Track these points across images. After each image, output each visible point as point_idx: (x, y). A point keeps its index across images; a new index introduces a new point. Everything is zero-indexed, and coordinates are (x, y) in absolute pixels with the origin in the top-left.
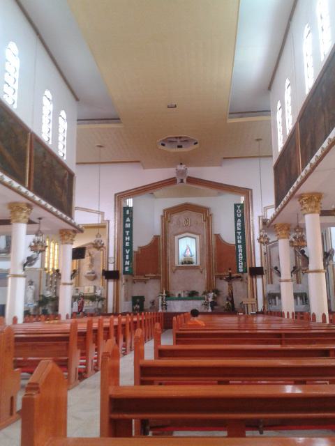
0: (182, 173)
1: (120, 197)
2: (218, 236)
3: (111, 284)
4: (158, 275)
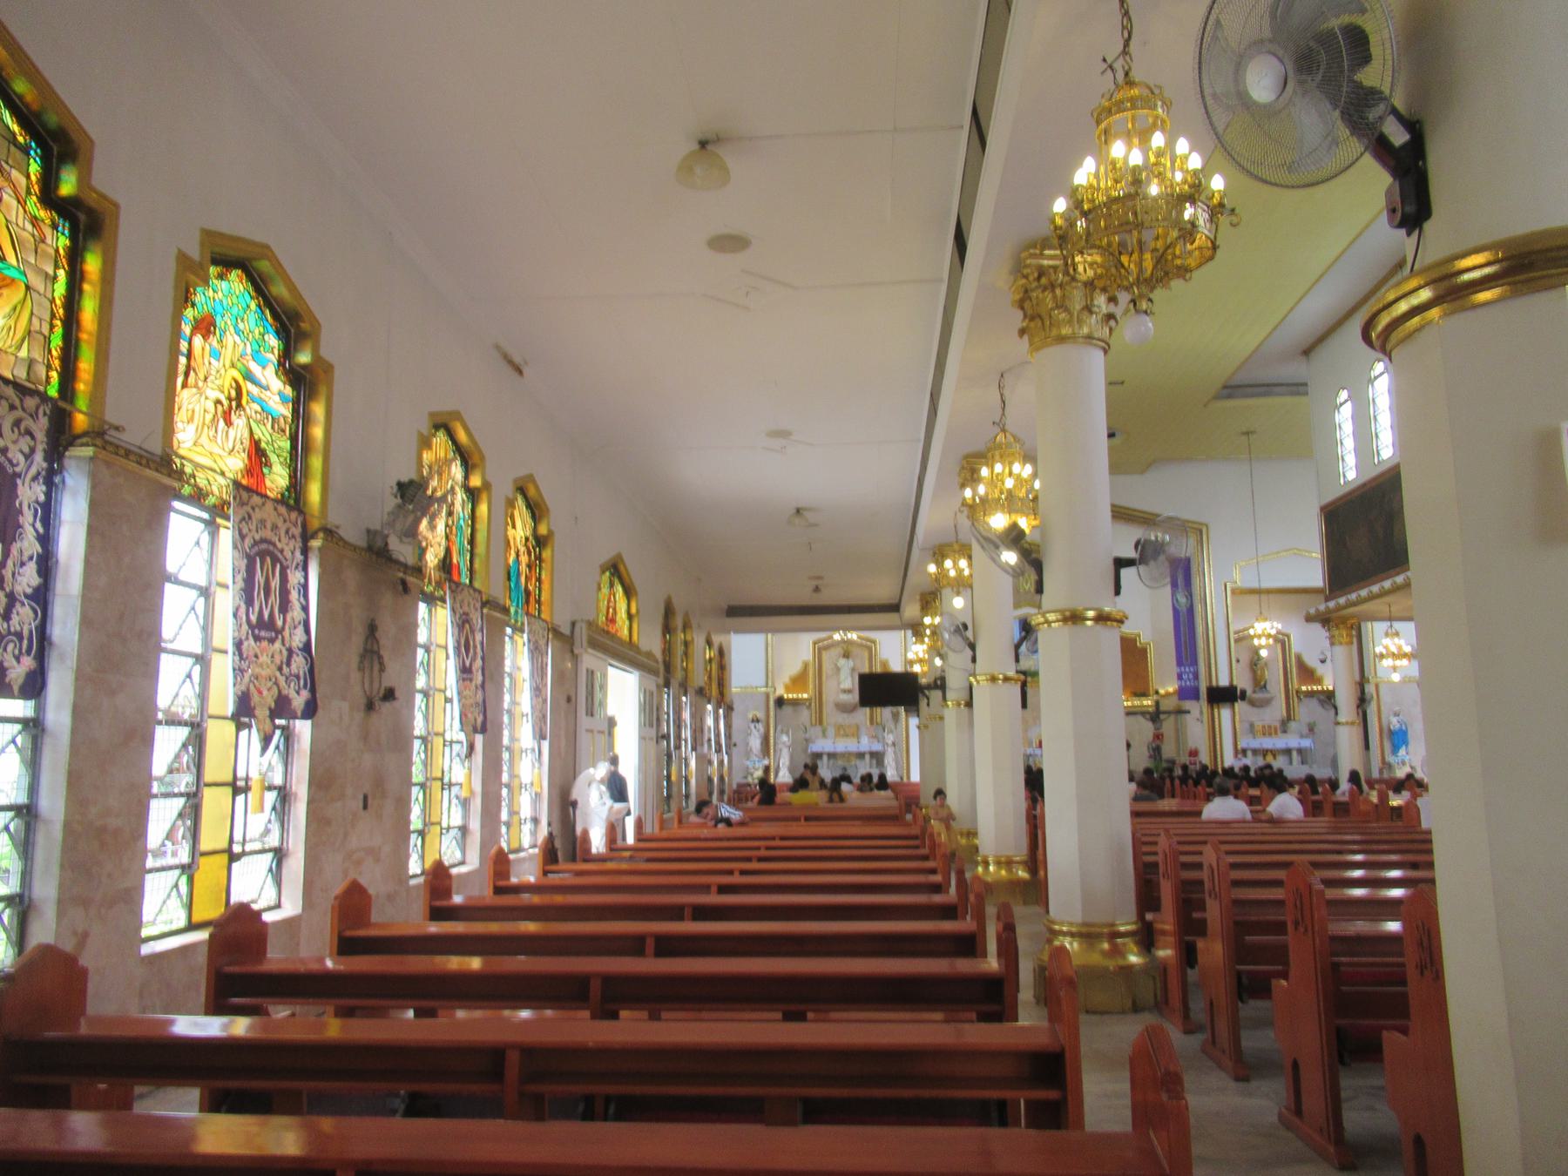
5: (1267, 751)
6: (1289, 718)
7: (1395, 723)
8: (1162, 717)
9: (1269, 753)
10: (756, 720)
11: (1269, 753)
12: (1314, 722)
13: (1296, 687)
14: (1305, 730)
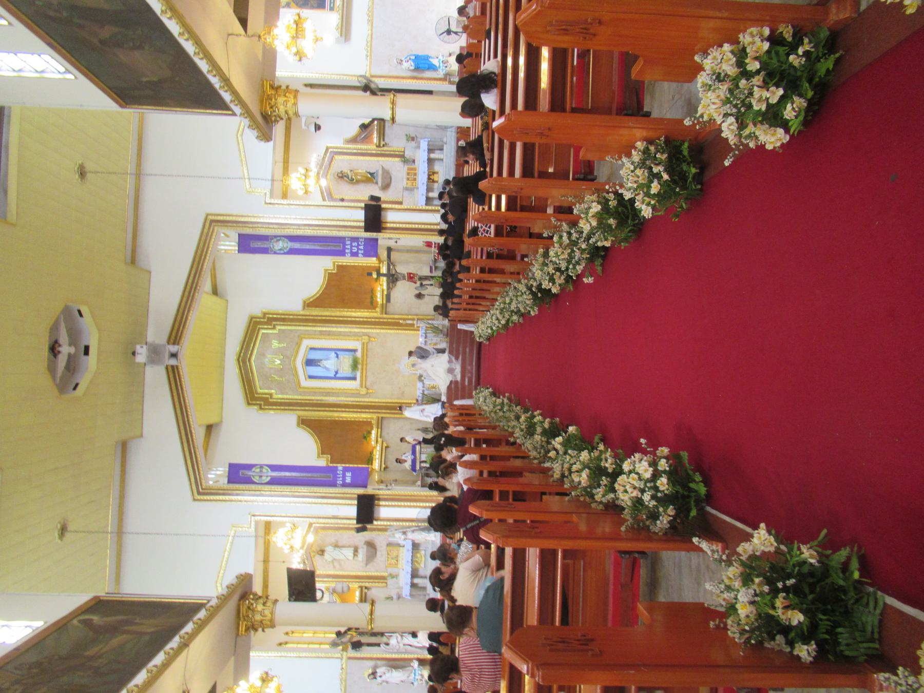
1: (201, 491)
2: (308, 304)
3: (384, 511)
4: (374, 422)
5: (429, 179)
6: (402, 156)
7: (410, 65)
10: (374, 674)
12: (406, 135)
13: (375, 147)
14: (413, 144)
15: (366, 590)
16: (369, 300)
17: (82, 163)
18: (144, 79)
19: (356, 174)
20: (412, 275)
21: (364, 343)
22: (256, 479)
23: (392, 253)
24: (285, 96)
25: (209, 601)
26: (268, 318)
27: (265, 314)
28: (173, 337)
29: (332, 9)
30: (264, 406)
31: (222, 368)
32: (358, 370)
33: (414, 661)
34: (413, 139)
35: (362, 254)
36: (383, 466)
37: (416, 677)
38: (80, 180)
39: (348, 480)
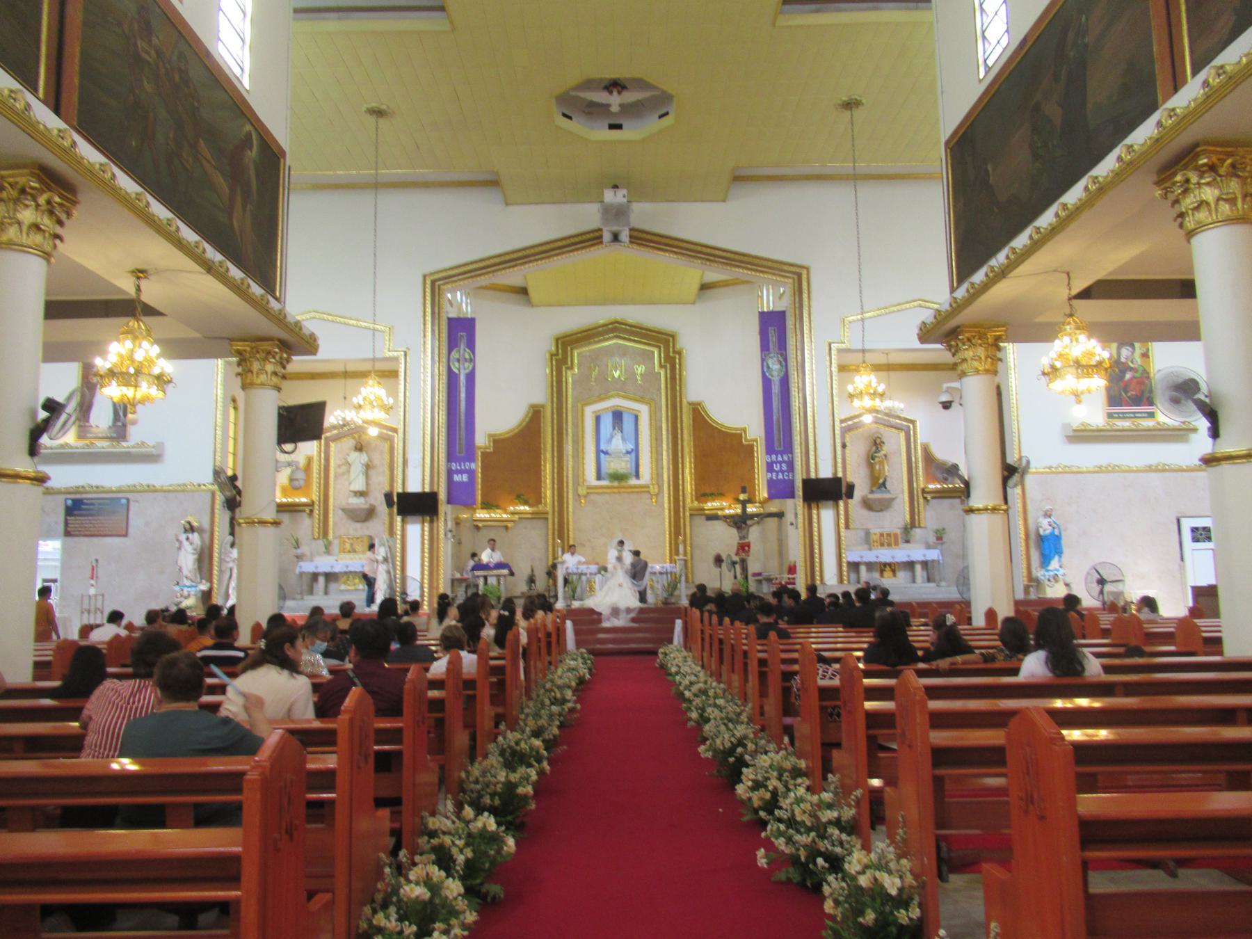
0: (619, 213)
3: (415, 531)
4: (541, 508)
5: (885, 565)
6: (913, 524)
7: (1045, 528)
8: (749, 522)
9: (888, 568)
10: (191, 529)
11: (888, 568)
12: (944, 529)
13: (922, 486)
14: (932, 539)
15: (308, 511)
16: (708, 492)
17: (863, 104)
18: (990, 168)
19: (881, 463)
20: (746, 548)
21: (649, 487)
22: (455, 354)
23: (776, 519)
24: (987, 357)
25: (276, 299)
26: (675, 358)
27: (680, 353)
28: (641, 235)
29: (1110, 416)
30: (557, 360)
31: (604, 302)
32: (610, 481)
33: (208, 584)
34: (939, 538)
35: (771, 478)
36: (480, 524)
37: (186, 589)
38: (840, 102)
39: (457, 478)
